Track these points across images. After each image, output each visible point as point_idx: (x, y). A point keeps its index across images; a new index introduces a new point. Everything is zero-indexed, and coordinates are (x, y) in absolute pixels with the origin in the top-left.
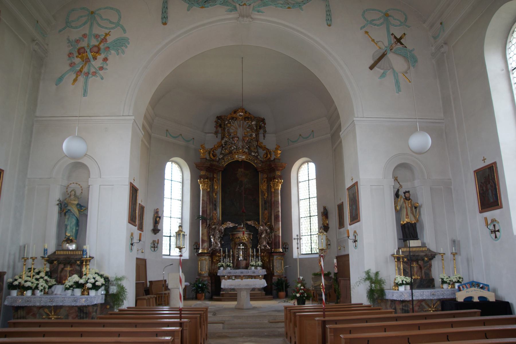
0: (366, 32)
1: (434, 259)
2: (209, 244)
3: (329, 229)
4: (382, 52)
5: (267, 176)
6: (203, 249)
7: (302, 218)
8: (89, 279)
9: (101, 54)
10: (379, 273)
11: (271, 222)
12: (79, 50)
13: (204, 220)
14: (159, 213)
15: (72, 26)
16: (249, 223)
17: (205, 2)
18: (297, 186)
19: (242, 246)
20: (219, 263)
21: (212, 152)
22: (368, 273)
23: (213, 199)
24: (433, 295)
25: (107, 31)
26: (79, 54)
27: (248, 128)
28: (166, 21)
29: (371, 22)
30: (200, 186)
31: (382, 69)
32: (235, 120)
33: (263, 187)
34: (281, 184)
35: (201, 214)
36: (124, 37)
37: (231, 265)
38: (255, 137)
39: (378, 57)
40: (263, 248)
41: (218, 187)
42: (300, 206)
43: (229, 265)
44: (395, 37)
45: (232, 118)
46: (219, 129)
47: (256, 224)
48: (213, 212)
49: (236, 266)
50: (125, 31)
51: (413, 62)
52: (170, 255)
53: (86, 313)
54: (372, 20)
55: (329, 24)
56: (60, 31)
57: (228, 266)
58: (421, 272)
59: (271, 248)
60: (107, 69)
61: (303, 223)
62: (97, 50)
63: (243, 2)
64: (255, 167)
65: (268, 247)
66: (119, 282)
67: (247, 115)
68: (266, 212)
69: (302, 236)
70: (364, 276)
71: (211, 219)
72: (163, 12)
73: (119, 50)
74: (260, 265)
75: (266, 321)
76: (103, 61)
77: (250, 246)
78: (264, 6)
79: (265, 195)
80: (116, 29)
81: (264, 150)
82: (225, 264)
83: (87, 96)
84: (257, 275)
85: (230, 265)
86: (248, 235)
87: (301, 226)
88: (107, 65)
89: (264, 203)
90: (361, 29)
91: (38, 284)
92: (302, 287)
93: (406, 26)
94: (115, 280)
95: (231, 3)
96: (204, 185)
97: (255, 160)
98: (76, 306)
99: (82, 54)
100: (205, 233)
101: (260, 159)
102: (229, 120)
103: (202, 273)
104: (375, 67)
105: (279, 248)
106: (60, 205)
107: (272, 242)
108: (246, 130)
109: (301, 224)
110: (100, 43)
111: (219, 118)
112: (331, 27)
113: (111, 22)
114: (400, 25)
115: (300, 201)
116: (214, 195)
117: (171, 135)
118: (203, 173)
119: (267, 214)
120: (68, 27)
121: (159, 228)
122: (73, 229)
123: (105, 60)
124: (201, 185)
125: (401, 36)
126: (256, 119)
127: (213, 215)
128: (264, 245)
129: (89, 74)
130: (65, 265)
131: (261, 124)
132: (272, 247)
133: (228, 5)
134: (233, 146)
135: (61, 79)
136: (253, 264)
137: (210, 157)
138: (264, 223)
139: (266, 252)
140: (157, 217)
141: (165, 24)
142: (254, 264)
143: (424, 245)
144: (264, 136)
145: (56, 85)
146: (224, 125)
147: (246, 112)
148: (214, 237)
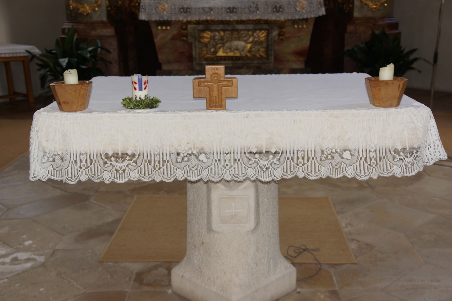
103: (81, 10)
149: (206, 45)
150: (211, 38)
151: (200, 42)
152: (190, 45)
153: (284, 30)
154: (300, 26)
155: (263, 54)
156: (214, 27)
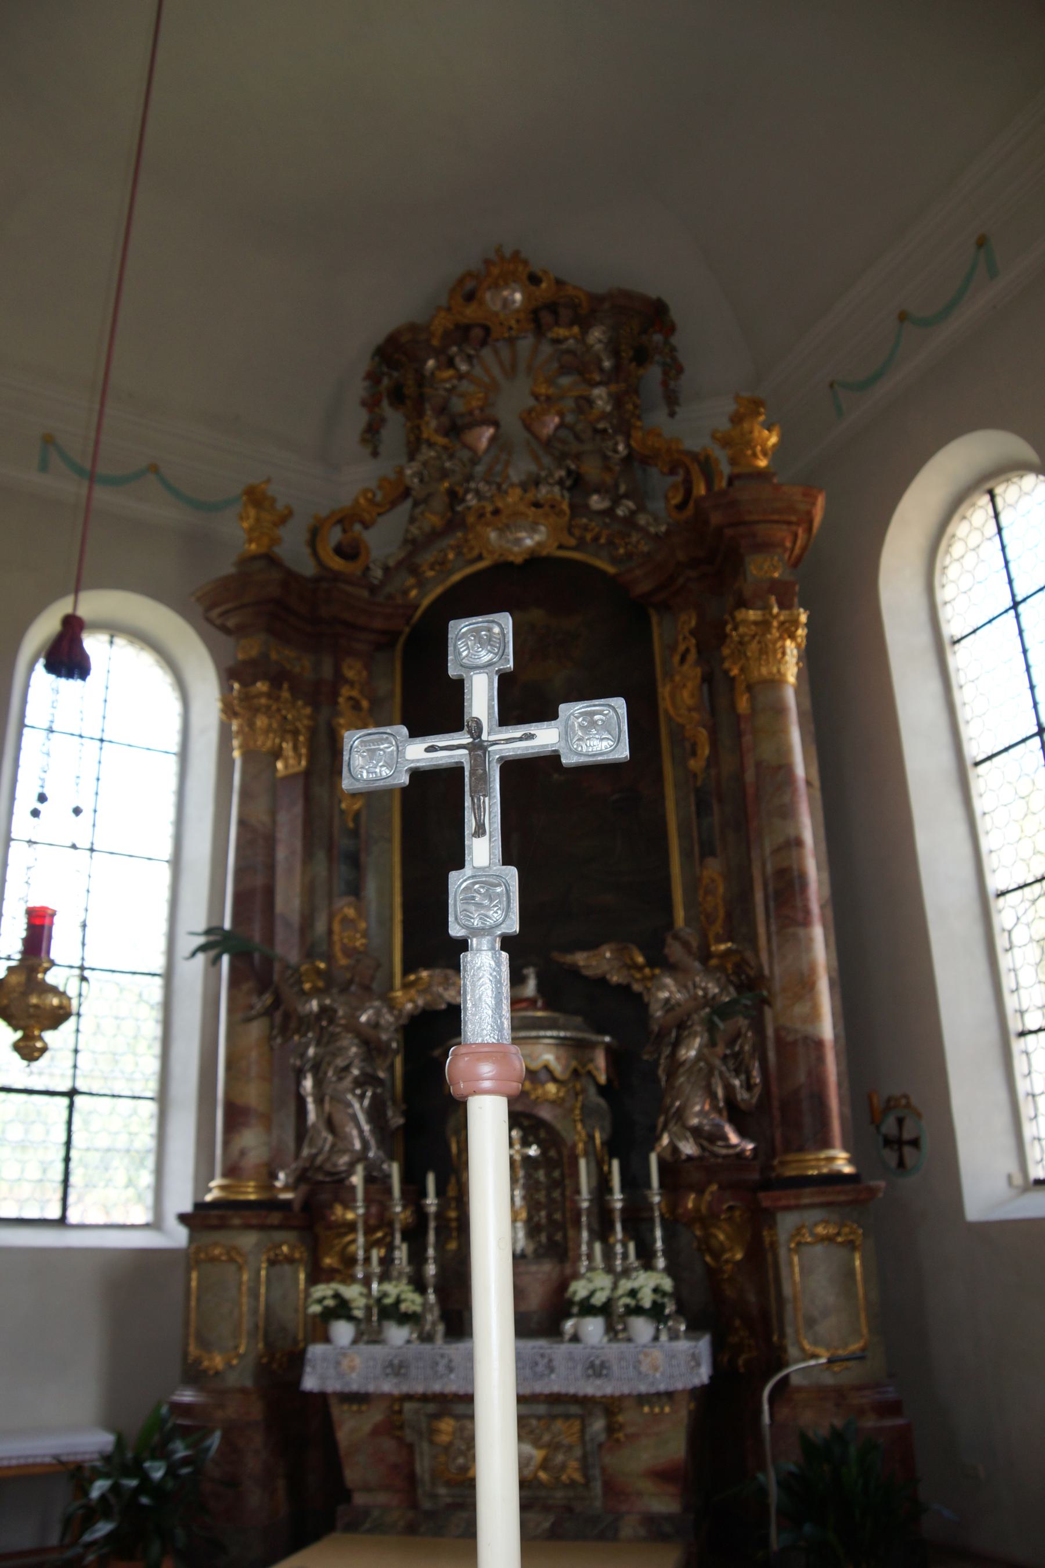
7: (1002, 894)
18: (934, 670)
32: (483, 343)
34: (792, 637)
35: (227, 925)
38: (609, 408)
47: (639, 968)
48: (330, 903)
52: (62, 1222)
57: (391, 1312)
61: (1020, 936)
65: (734, 1138)
68: (713, 869)
69: (1022, 1034)
74: (647, 1303)
77: (591, 1137)
79: (694, 753)
84: (626, 1390)
85: (403, 1307)
86: (562, 1052)
87: (1005, 962)
89: (693, 808)
100: (254, 1055)
105: (826, 1143)
109: (1001, 942)
115: (972, 773)
118: (251, 648)
126: (606, 306)
127: (330, 932)
134: (473, 485)
136: (592, 1293)
139: (714, 1187)
147: (534, 279)
150: (454, 1433)
151: (431, 1442)
152: (410, 1448)
153: (620, 1418)
154: (657, 1410)
155: (577, 1476)
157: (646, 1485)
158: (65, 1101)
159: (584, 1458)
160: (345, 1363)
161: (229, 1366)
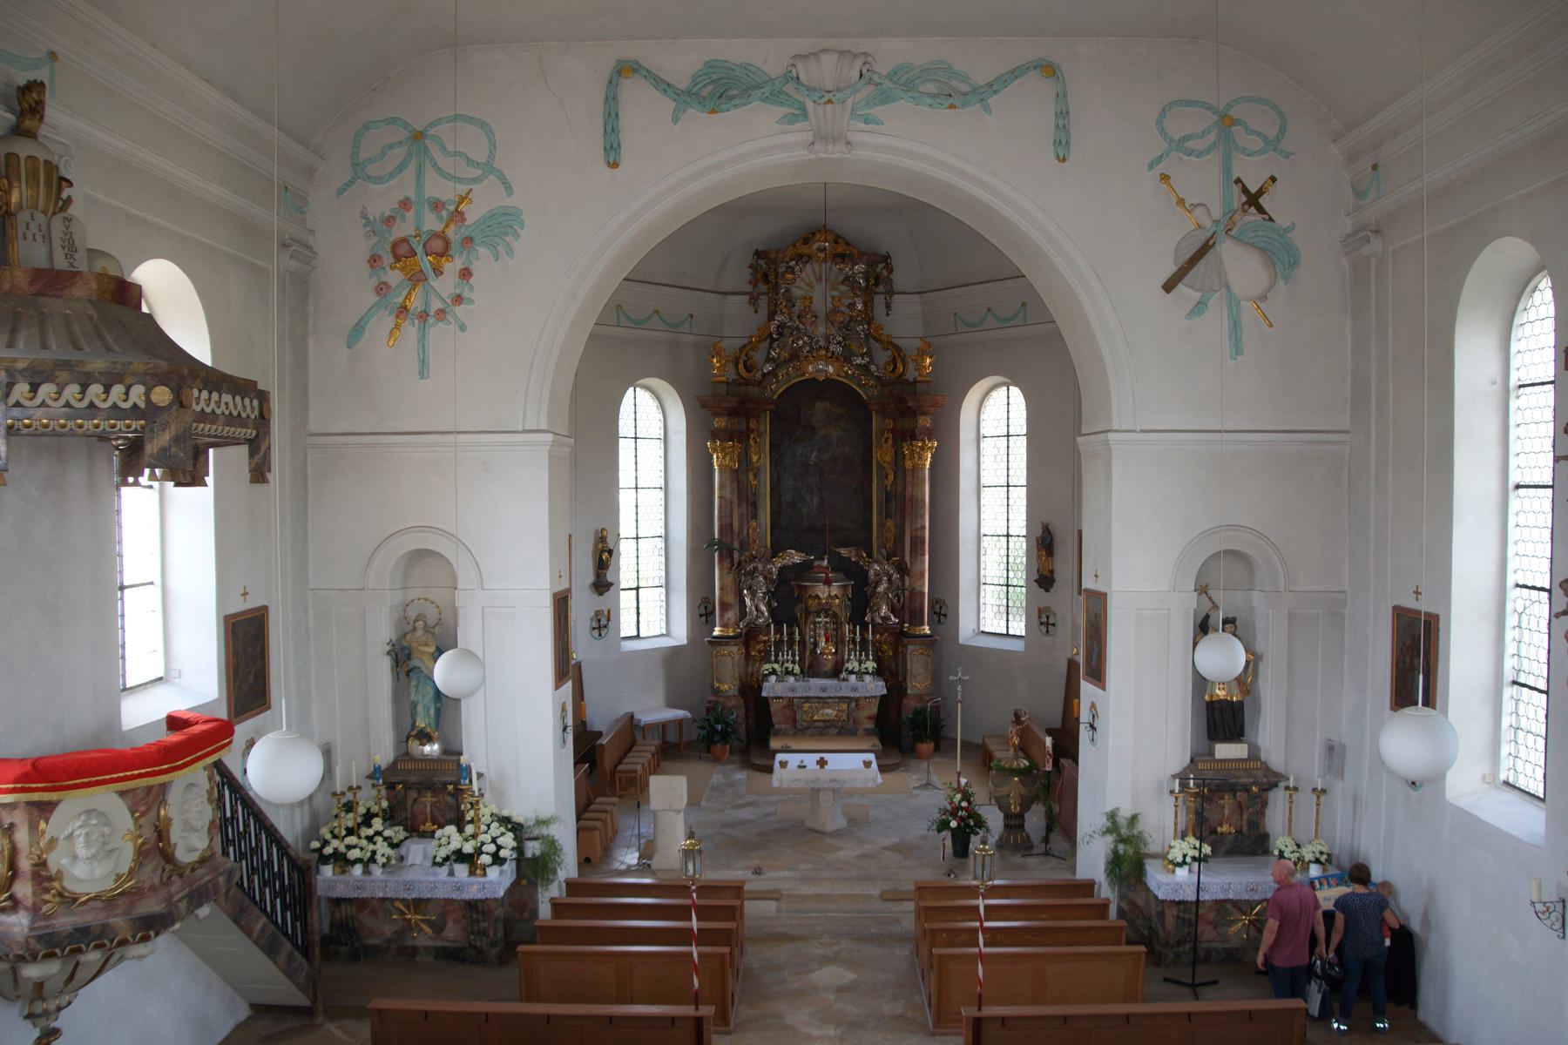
0: (1165, 178)
1: (1275, 789)
2: (740, 611)
3: (1055, 584)
4: (1202, 236)
5: (895, 425)
6: (724, 626)
8: (483, 844)
9: (452, 257)
10: (1139, 817)
11: (903, 557)
12: (395, 246)
13: (726, 552)
14: (608, 540)
15: (368, 177)
16: (843, 552)
17: (720, 97)
19: (825, 617)
20: (767, 666)
21: (742, 358)
22: (1112, 816)
23: (747, 489)
24: (1252, 890)
25: (462, 189)
26: (398, 258)
27: (843, 283)
28: (617, 158)
29: (1180, 145)
30: (713, 459)
31: (1196, 290)
32: (808, 262)
33: (882, 454)
35: (716, 537)
36: (507, 207)
37: (797, 669)
39: (1188, 256)
40: (880, 621)
41: (762, 458)
42: (982, 502)
43: (790, 669)
44: (1245, 190)
45: (799, 258)
46: (763, 288)
48: (748, 523)
49: (809, 667)
50: (511, 188)
51: (1287, 267)
52: (638, 636)
53: (483, 912)
54: (1184, 137)
55: (1061, 157)
56: (340, 192)
57: (788, 673)
58: (1241, 815)
59: (902, 622)
60: (471, 301)
62: (442, 250)
63: (824, 96)
64: (862, 397)
66: (545, 831)
67: (840, 249)
68: (890, 523)
70: (1103, 822)
71: (744, 546)
72: (609, 130)
73: (498, 245)
74: (870, 672)
75: (875, 891)
76: (460, 277)
78: (882, 102)
79: (887, 478)
80: (485, 182)
81: (887, 350)
82: (782, 667)
83: (428, 377)
87: (982, 558)
88: (472, 289)
90: (1151, 166)
91: (374, 853)
92: (964, 804)
93: (1282, 152)
94: (534, 825)
95: (790, 97)
96: (724, 458)
97: (863, 377)
98: (461, 900)
99: (403, 259)
101: (876, 374)
102: (791, 260)
104: (1180, 284)
105: (923, 625)
106: (393, 653)
107: (903, 605)
108: (836, 289)
109: (982, 552)
110: (447, 226)
111: (759, 254)
112: (1067, 163)
113: (470, 162)
114: (1262, 151)
115: (982, 489)
116: (751, 476)
117: (630, 320)
118: (719, 423)
119: (893, 529)
120: (360, 178)
121: (610, 578)
122: (429, 709)
123: (466, 274)
124: (715, 457)
125: (1261, 188)
126: (866, 257)
128: (882, 614)
129: (428, 315)
130: (419, 792)
131: (879, 270)
132: (904, 619)
133: (782, 104)
135: (358, 330)
137: (738, 373)
138: (883, 556)
140: (603, 551)
141: (615, 165)
142: (856, 669)
143: (1254, 754)
144: (888, 307)
145: (348, 346)
146: (776, 277)
148: (753, 594)
149: (806, 712)
153: (860, 703)
156: (811, 701)
157: (865, 721)
158: (635, 591)
159: (848, 714)
160: (776, 688)
161: (730, 688)
